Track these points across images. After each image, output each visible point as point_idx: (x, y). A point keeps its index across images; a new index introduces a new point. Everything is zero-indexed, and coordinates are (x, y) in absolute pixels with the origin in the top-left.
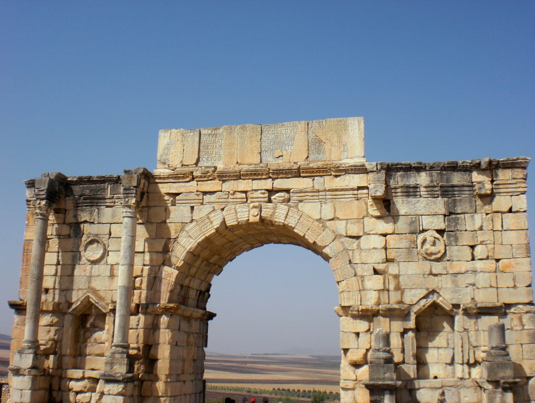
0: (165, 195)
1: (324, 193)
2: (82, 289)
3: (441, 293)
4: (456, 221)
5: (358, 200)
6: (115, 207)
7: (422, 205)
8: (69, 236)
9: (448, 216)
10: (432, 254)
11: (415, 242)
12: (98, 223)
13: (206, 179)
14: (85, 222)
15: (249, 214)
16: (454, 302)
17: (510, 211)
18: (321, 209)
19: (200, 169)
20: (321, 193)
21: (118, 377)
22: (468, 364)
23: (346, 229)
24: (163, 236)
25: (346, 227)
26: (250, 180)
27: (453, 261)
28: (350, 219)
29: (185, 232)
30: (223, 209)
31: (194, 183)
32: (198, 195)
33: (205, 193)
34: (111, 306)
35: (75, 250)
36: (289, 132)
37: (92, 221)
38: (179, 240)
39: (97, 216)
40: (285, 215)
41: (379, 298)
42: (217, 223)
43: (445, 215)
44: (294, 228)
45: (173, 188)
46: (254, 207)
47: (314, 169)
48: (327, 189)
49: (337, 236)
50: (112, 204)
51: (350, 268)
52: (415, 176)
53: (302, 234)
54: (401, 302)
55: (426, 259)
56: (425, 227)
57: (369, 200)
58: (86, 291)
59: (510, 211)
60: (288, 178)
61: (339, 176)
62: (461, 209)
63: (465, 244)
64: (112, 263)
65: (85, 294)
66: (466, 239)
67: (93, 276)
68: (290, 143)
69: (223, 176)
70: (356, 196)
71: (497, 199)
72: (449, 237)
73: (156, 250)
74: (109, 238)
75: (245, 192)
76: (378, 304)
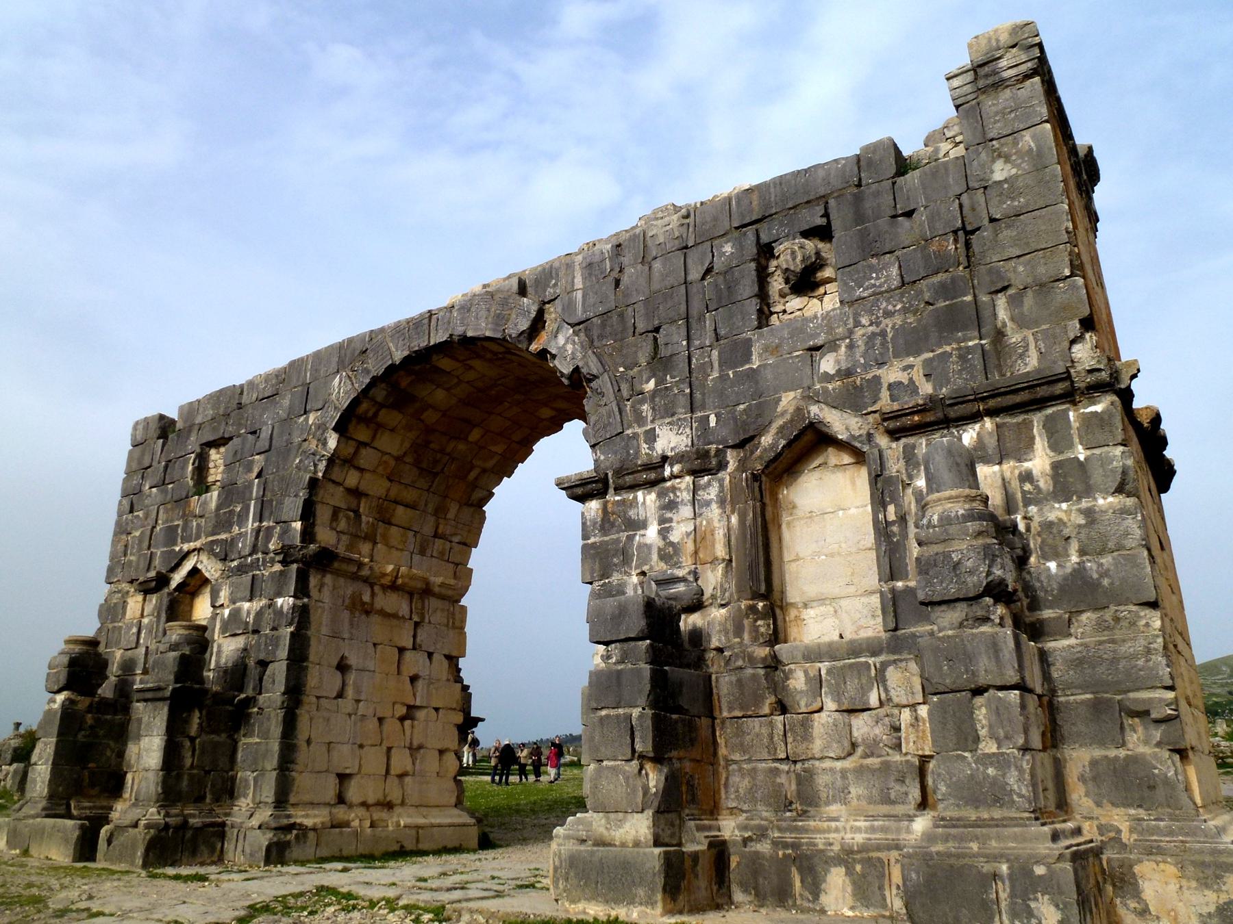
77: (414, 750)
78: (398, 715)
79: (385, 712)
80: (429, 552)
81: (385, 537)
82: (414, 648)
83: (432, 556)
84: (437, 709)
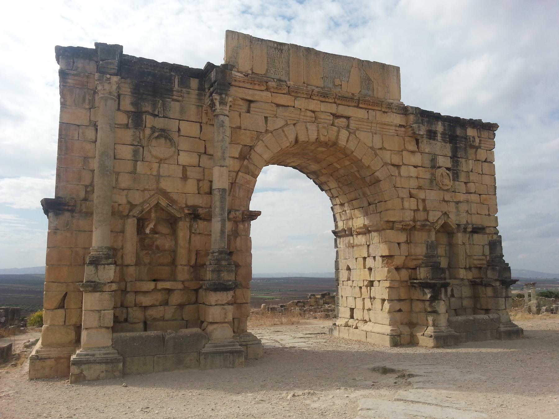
0: (239, 99)
1: (375, 125)
2: (148, 190)
3: (450, 216)
4: (457, 162)
5: (397, 135)
6: (184, 102)
7: (438, 147)
8: (127, 126)
9: (452, 158)
10: (446, 185)
11: (433, 174)
12: (164, 117)
13: (280, 92)
14: (147, 112)
15: (318, 133)
16: (457, 223)
17: (486, 161)
18: (373, 139)
19: (272, 80)
20: (373, 125)
21: (230, 285)
22: (465, 268)
23: (391, 158)
24: (239, 142)
25: (391, 157)
26: (319, 102)
27: (456, 192)
28: (393, 150)
29: (260, 142)
30: (294, 124)
31: (268, 94)
32: (272, 106)
33: (278, 105)
34: (188, 210)
35: (136, 144)
36: (345, 64)
37: (156, 113)
38: (256, 149)
39: (162, 109)
40: (346, 140)
41: (414, 216)
42: (292, 138)
43: (450, 157)
44: (353, 152)
45: (249, 94)
46: (324, 127)
47: (370, 102)
48: (378, 122)
49: (385, 164)
50: (180, 98)
51: (395, 191)
52: (435, 124)
53: (360, 158)
54: (427, 220)
55: (440, 189)
56: (441, 165)
57: (405, 137)
58: (153, 192)
59: (485, 161)
60: (349, 106)
61: (386, 112)
62: (460, 155)
63: (462, 181)
64: (184, 164)
65: (153, 195)
66: (463, 177)
67: (162, 176)
68: (346, 75)
69: (296, 92)
70: (397, 132)
71: (479, 150)
72: (453, 174)
73: (232, 155)
74: (179, 136)
75: (314, 112)
76: (414, 220)
77: (372, 299)
78: (365, 285)
79: (361, 285)
80: (369, 214)
81: (354, 215)
82: (369, 256)
83: (371, 214)
84: (379, 281)
